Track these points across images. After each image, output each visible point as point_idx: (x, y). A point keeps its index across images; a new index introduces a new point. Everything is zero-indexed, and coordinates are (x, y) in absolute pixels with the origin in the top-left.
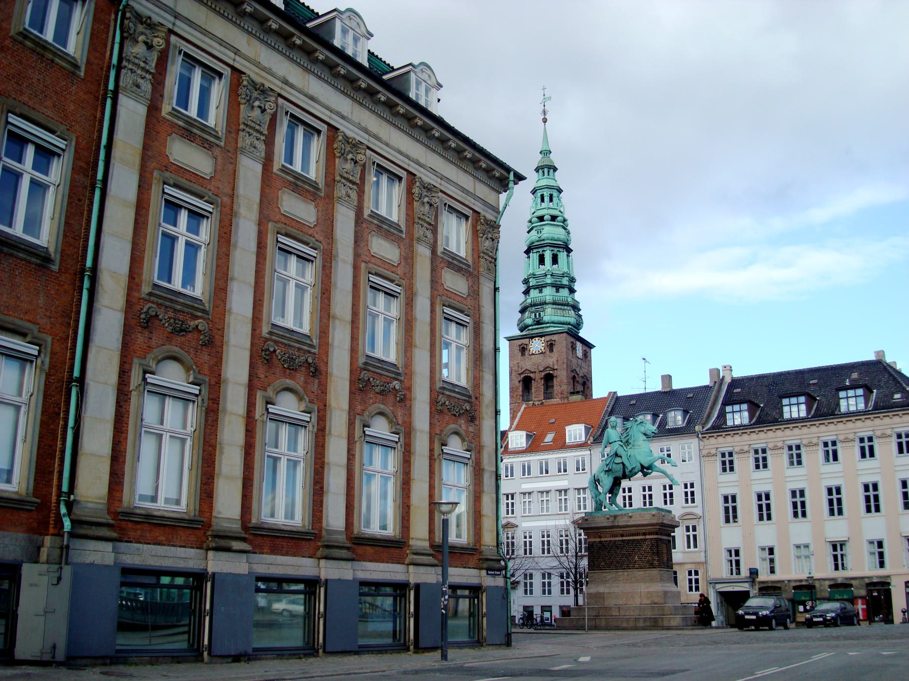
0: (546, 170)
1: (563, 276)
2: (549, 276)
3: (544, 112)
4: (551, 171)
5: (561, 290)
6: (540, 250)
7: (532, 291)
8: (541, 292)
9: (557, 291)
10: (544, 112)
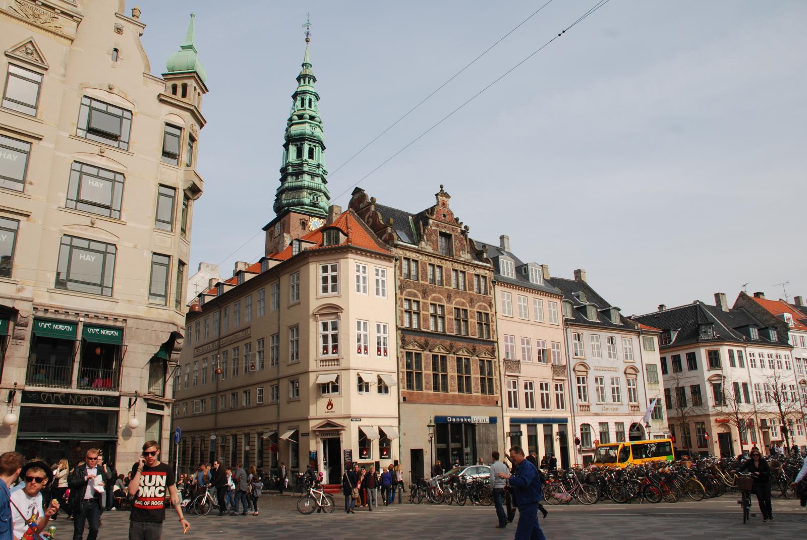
0: (307, 79)
1: (318, 166)
2: (305, 165)
3: (308, 34)
4: (312, 80)
5: (316, 179)
6: (299, 143)
7: (289, 179)
8: (297, 178)
9: (312, 178)
10: (308, 34)
